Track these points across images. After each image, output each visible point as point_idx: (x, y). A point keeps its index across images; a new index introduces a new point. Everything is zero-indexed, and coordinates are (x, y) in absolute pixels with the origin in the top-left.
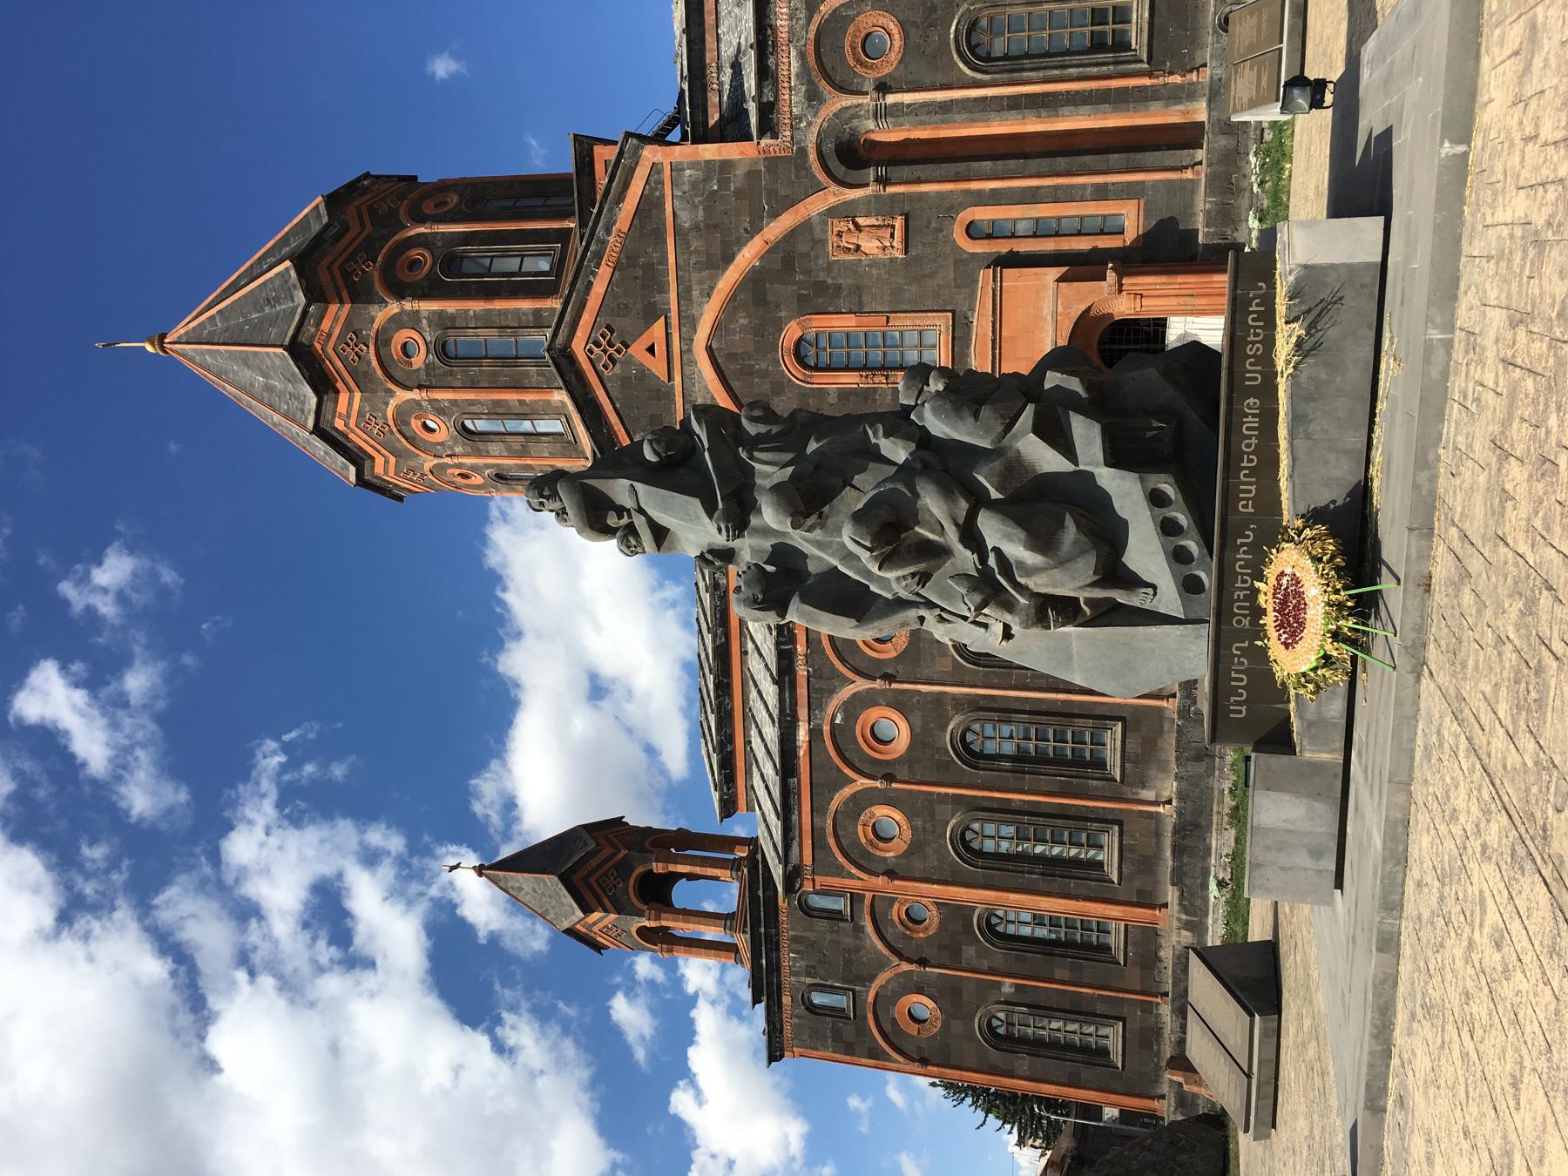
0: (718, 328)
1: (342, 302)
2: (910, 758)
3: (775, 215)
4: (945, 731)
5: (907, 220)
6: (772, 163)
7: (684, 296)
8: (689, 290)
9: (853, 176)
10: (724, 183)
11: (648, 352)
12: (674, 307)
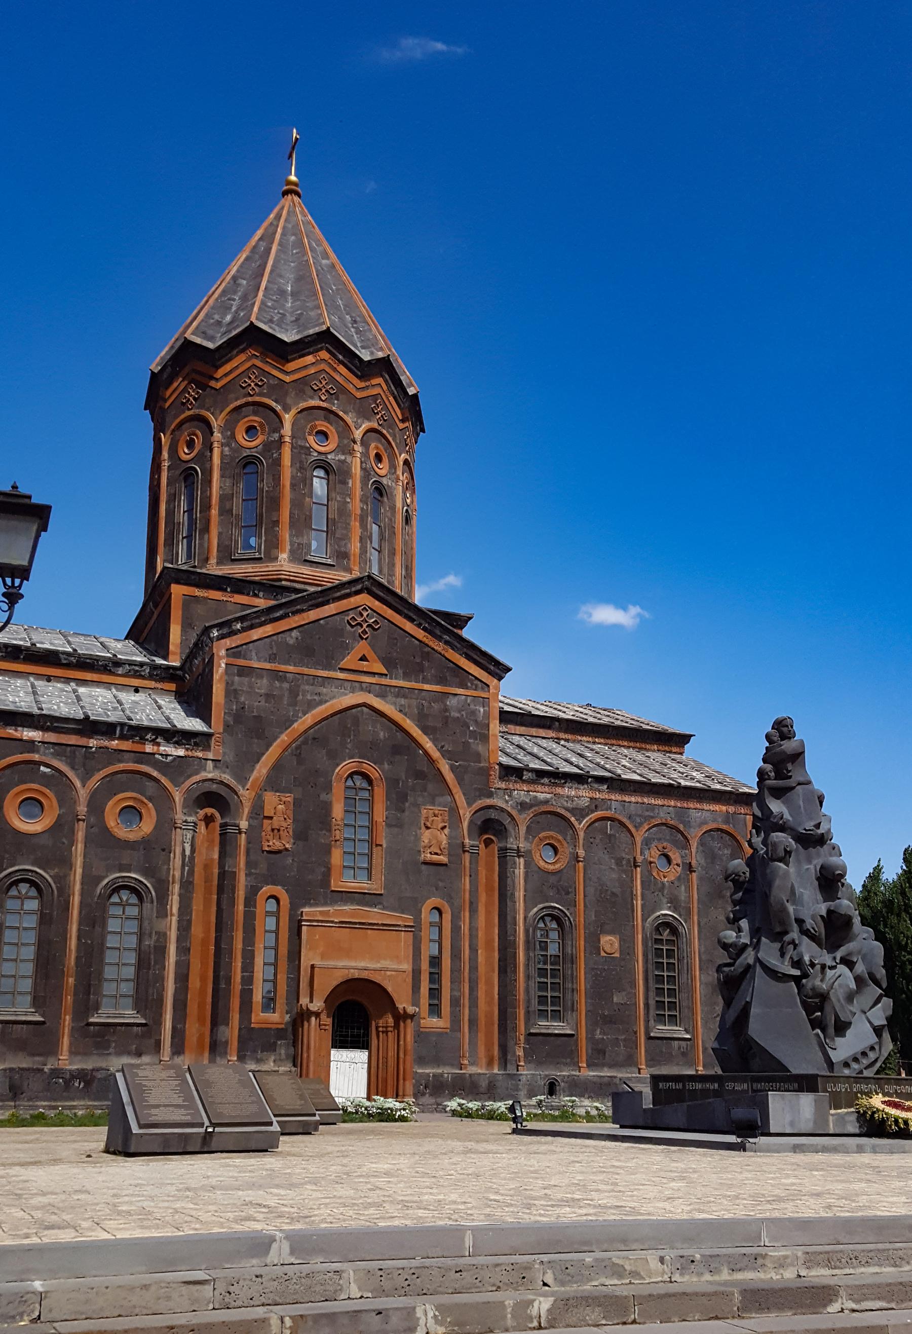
3: (453, 769)
4: (33, 865)
5: (446, 865)
6: (485, 773)
7: (401, 692)
8: (405, 697)
10: (473, 734)
12: (394, 682)
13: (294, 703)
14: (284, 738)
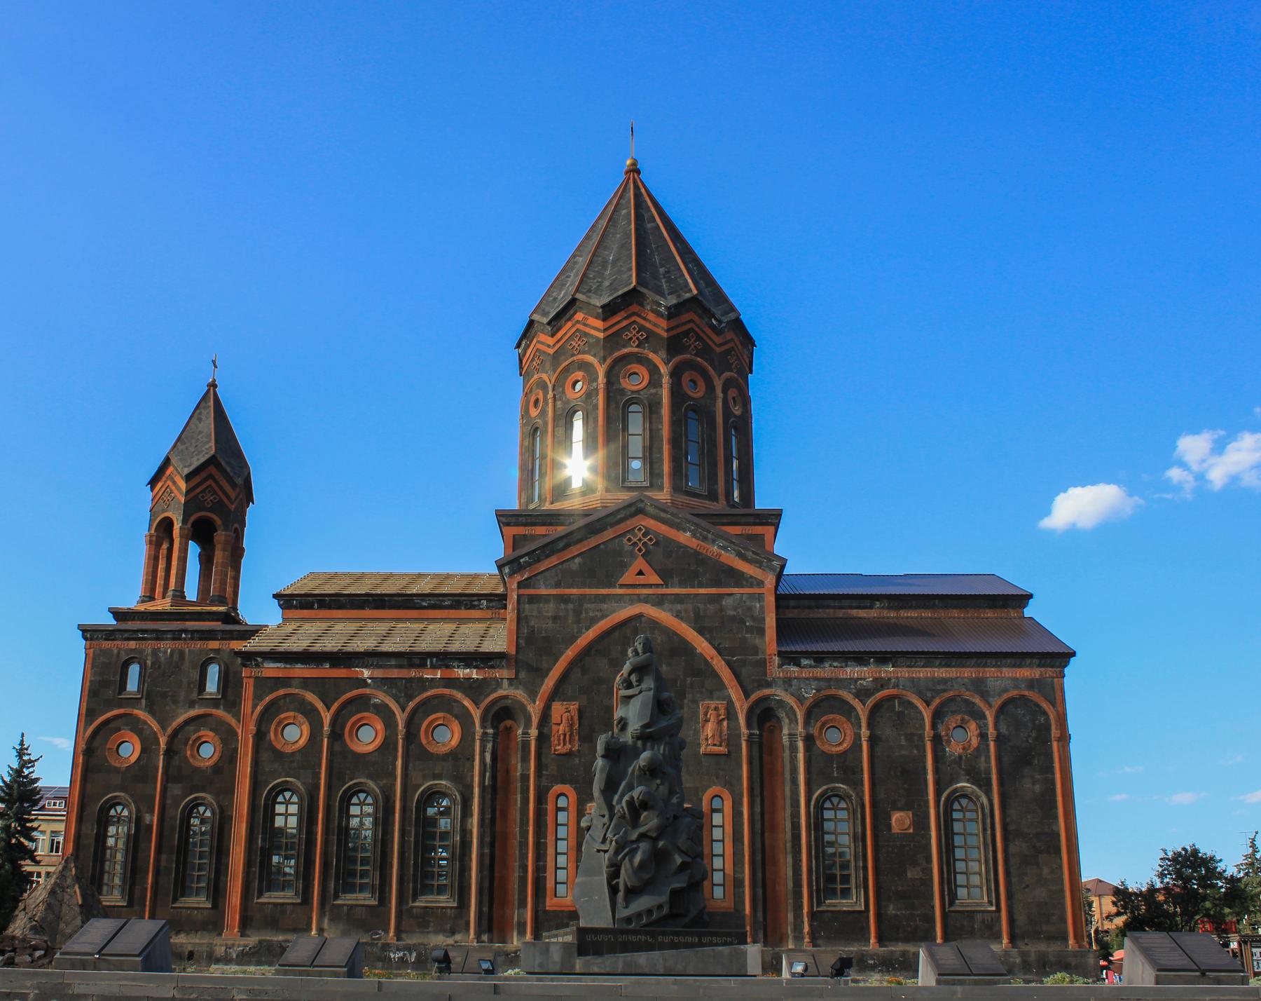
0: (654, 625)
1: (668, 331)
2: (347, 753)
3: (729, 664)
6: (762, 664)
7: (678, 599)
9: (755, 719)
11: (639, 573)
13: (578, 621)
14: (570, 653)
